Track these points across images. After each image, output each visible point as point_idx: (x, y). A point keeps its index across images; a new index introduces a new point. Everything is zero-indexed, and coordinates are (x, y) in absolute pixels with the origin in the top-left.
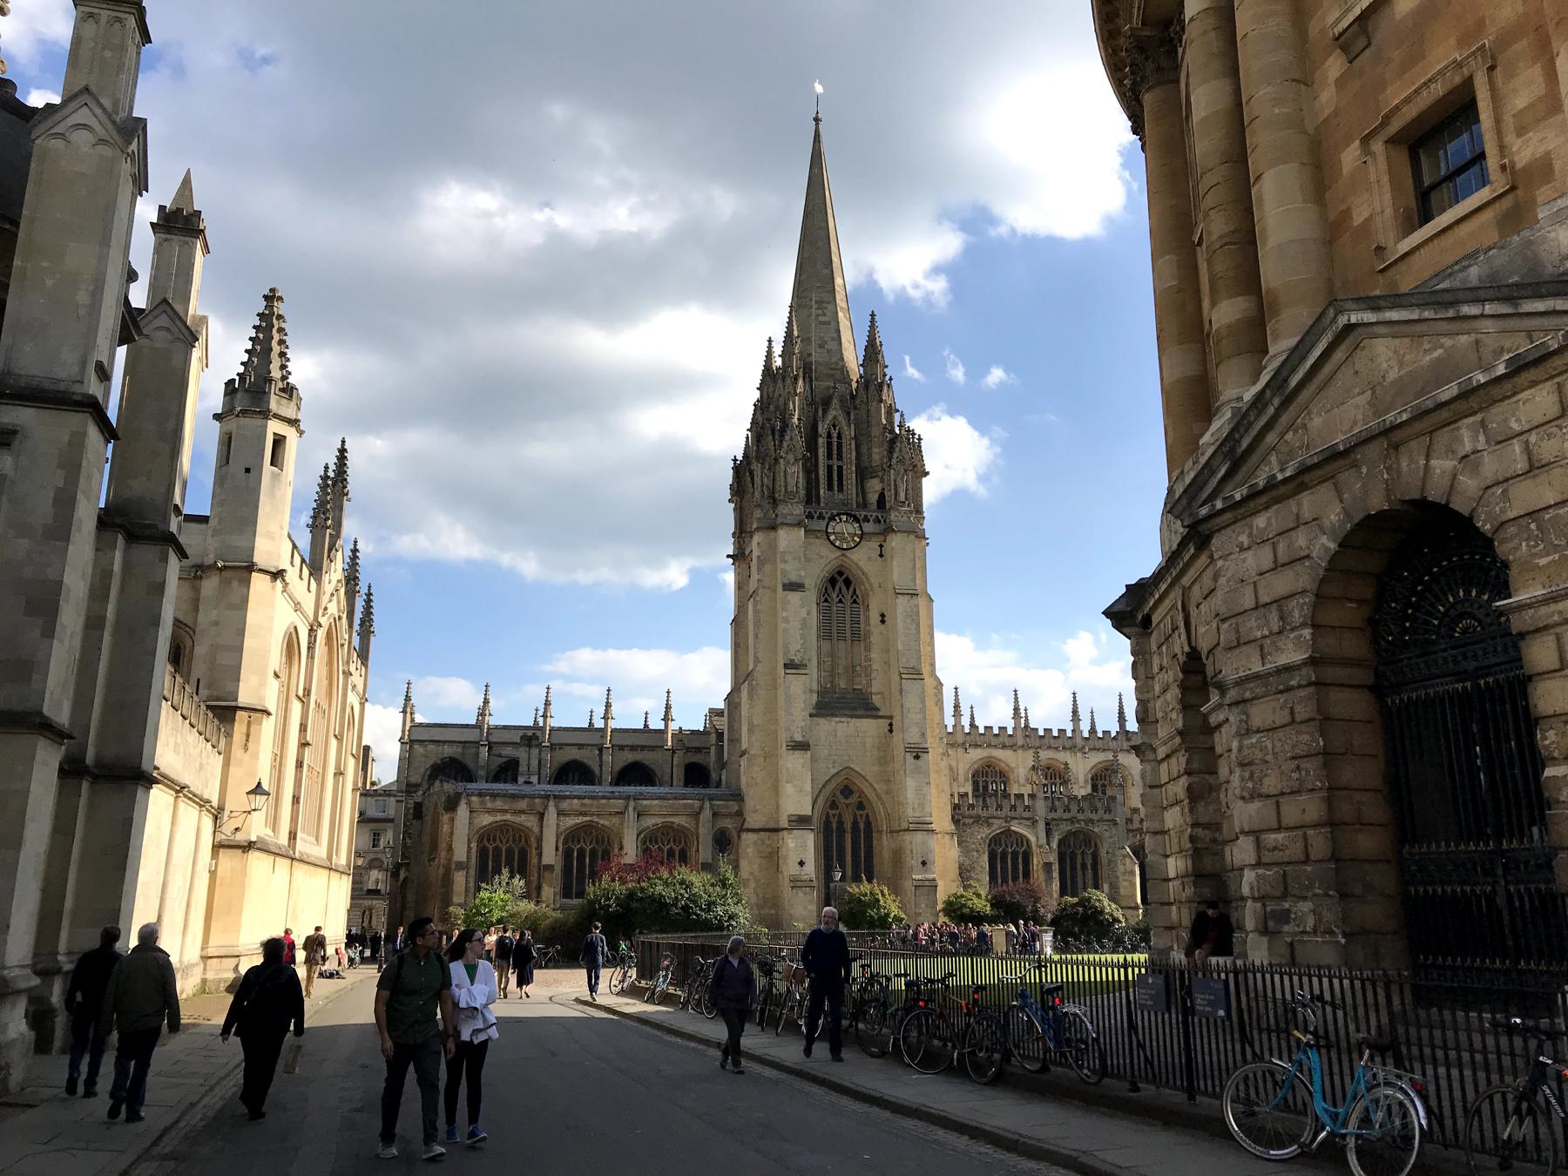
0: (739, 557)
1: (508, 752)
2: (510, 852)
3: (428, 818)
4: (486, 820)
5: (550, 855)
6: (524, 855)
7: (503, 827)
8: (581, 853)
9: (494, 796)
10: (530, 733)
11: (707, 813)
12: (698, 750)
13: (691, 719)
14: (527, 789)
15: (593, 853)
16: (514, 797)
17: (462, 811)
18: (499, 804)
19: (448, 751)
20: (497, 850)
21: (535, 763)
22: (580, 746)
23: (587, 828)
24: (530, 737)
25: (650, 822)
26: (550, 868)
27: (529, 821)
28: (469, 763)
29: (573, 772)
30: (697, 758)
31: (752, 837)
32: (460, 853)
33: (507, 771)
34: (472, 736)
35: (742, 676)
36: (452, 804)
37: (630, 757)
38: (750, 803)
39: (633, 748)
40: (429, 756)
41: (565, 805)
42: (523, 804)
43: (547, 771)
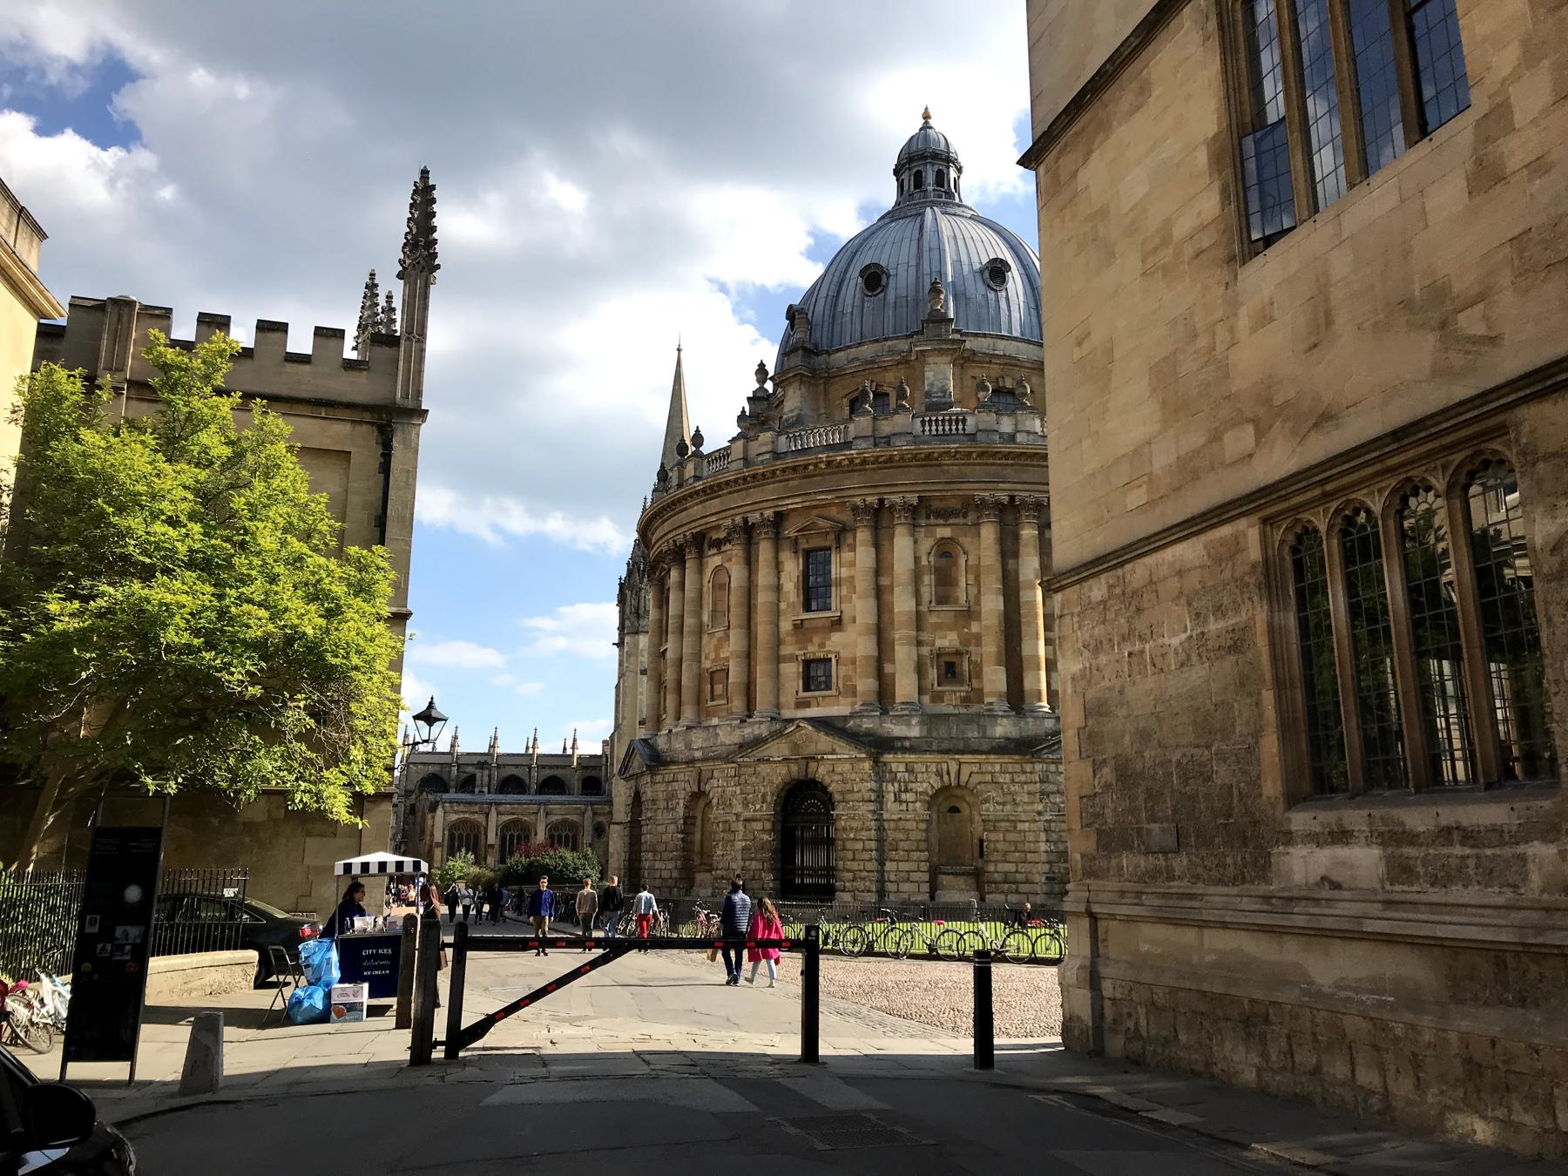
0: (620, 645)
1: (470, 769)
2: (468, 836)
3: (419, 814)
4: (454, 817)
5: (492, 838)
6: (477, 838)
7: (465, 821)
8: (512, 837)
9: (459, 803)
10: (483, 759)
11: (589, 813)
12: (594, 768)
13: (591, 746)
14: (478, 798)
15: (519, 838)
16: (470, 803)
17: (440, 812)
18: (462, 807)
19: (431, 769)
20: (460, 836)
21: (486, 779)
22: (517, 766)
23: (515, 822)
24: (483, 762)
25: (554, 818)
26: (492, 846)
27: (480, 818)
28: (445, 777)
29: (512, 784)
30: (593, 773)
31: (616, 827)
32: (438, 837)
33: (468, 784)
34: (447, 759)
35: (617, 727)
36: (433, 808)
37: (548, 773)
38: (616, 807)
39: (551, 767)
40: (419, 773)
41: (502, 808)
42: (476, 808)
43: (494, 782)
